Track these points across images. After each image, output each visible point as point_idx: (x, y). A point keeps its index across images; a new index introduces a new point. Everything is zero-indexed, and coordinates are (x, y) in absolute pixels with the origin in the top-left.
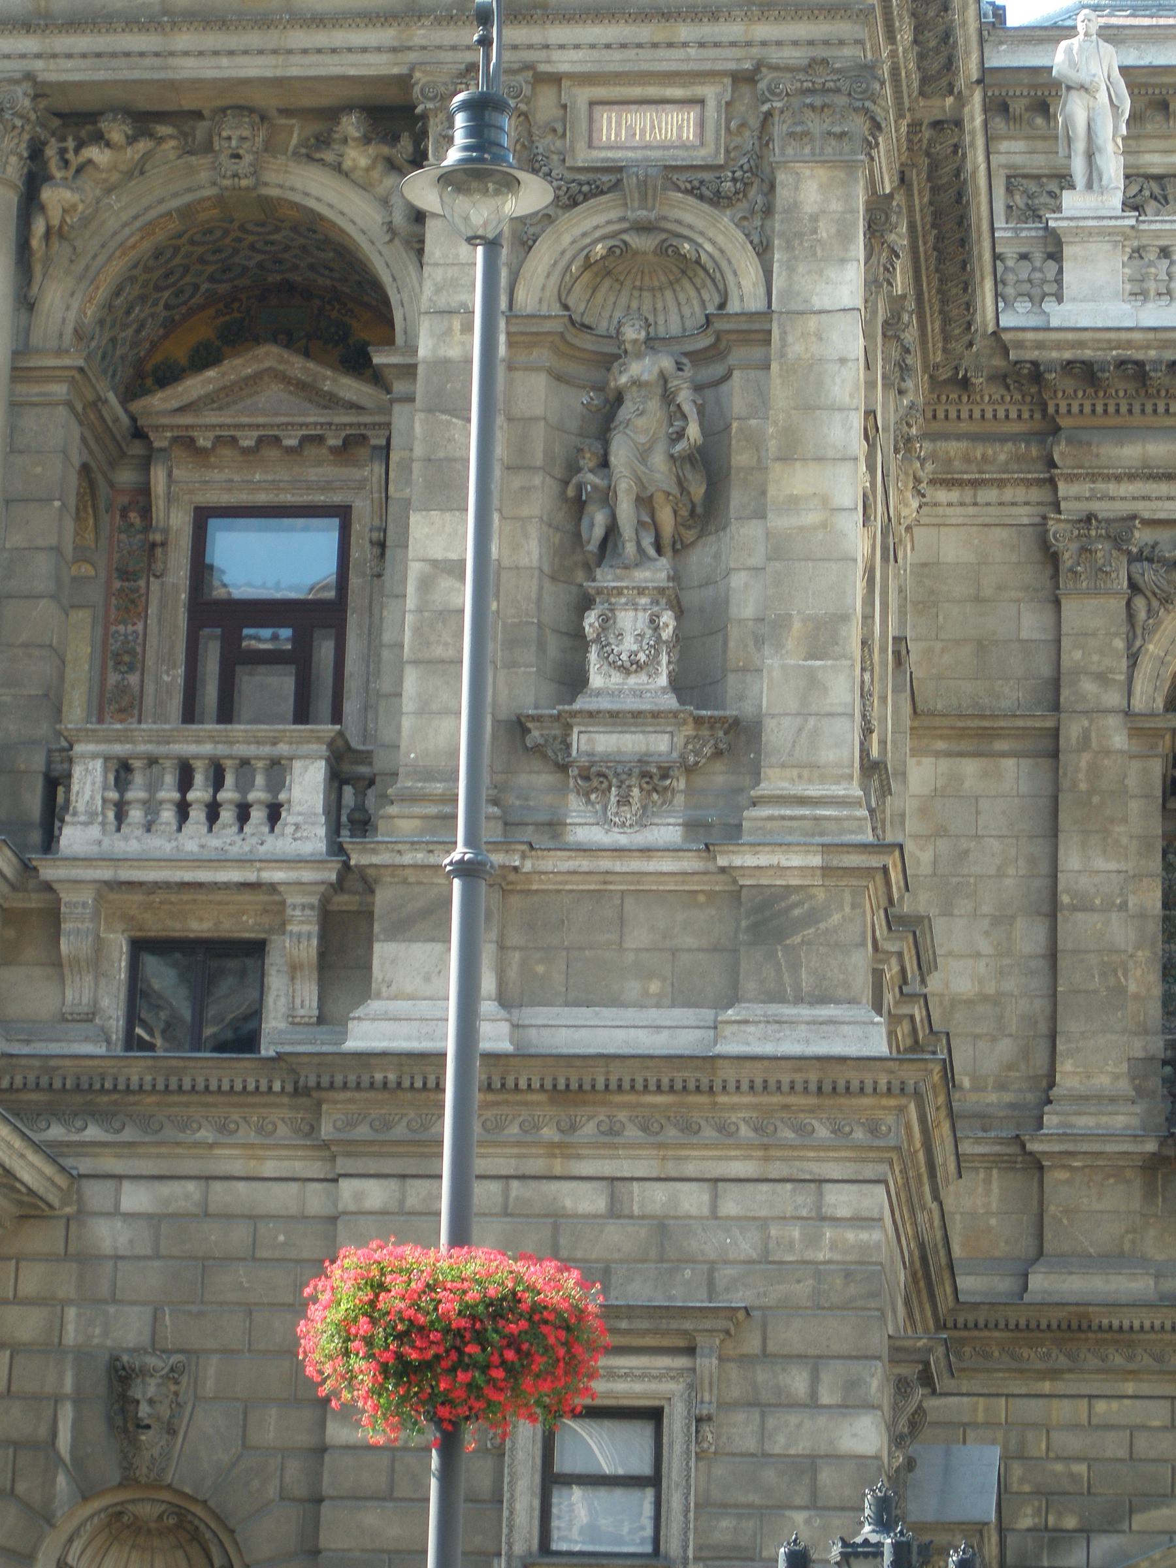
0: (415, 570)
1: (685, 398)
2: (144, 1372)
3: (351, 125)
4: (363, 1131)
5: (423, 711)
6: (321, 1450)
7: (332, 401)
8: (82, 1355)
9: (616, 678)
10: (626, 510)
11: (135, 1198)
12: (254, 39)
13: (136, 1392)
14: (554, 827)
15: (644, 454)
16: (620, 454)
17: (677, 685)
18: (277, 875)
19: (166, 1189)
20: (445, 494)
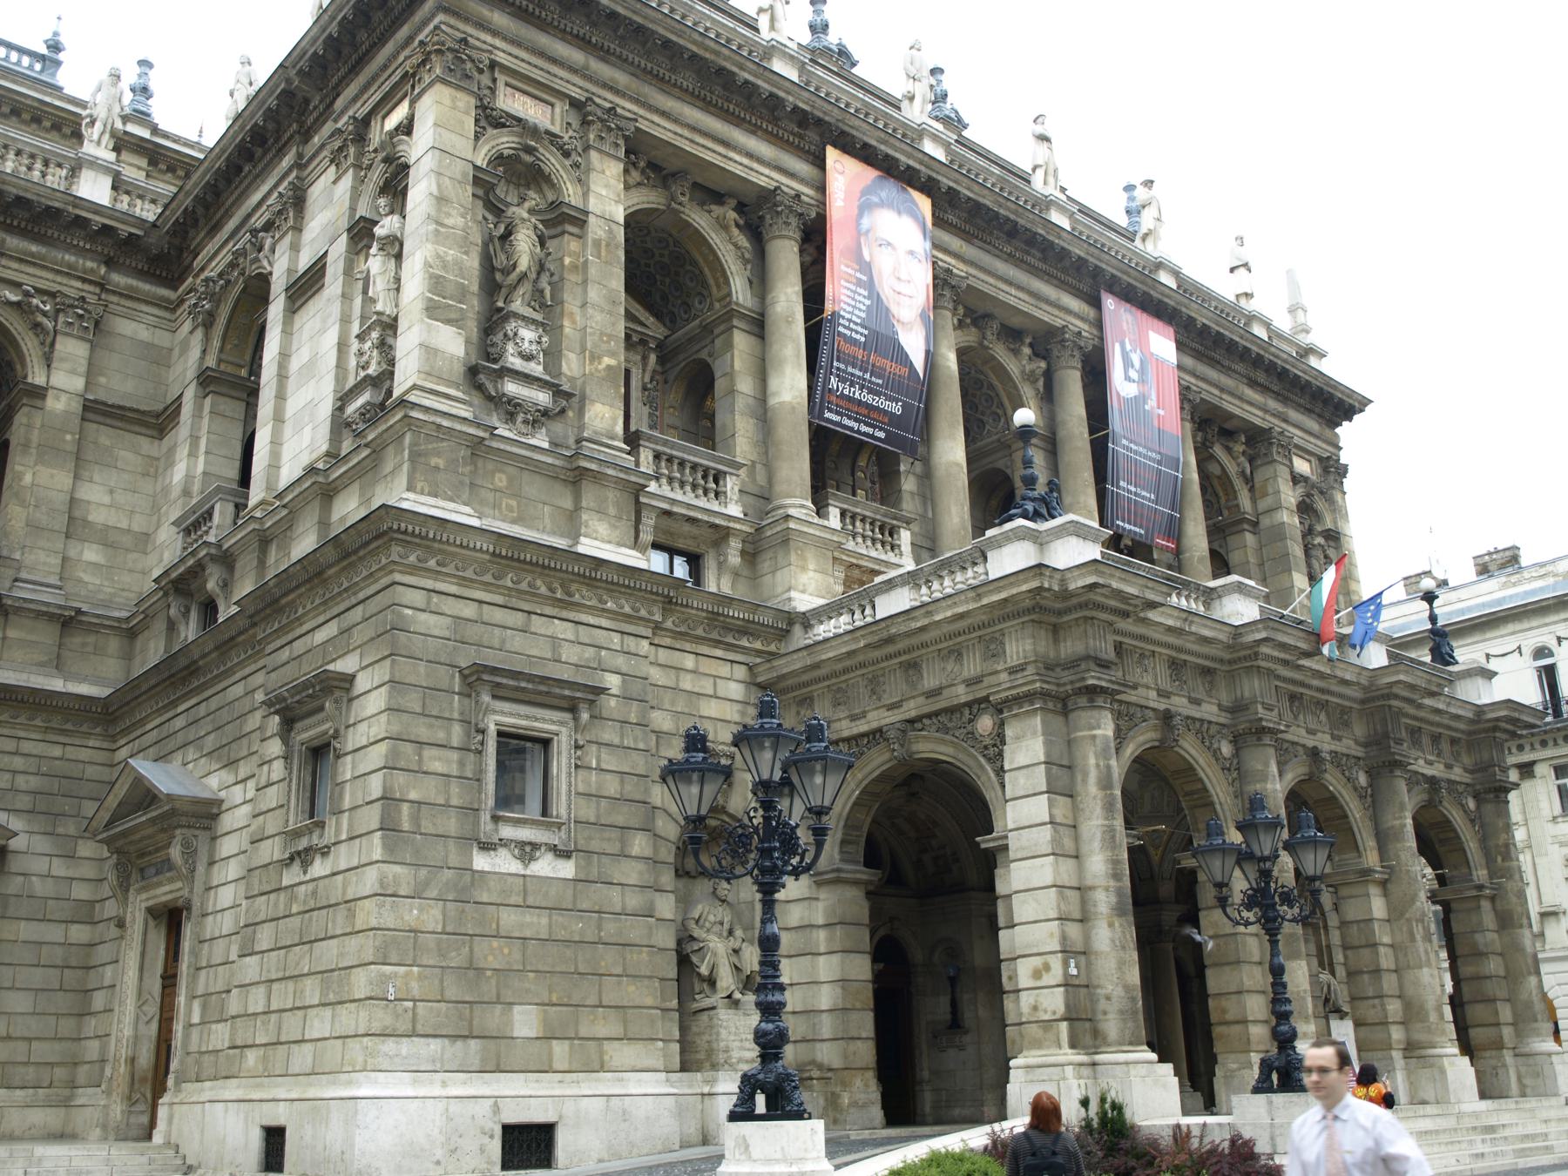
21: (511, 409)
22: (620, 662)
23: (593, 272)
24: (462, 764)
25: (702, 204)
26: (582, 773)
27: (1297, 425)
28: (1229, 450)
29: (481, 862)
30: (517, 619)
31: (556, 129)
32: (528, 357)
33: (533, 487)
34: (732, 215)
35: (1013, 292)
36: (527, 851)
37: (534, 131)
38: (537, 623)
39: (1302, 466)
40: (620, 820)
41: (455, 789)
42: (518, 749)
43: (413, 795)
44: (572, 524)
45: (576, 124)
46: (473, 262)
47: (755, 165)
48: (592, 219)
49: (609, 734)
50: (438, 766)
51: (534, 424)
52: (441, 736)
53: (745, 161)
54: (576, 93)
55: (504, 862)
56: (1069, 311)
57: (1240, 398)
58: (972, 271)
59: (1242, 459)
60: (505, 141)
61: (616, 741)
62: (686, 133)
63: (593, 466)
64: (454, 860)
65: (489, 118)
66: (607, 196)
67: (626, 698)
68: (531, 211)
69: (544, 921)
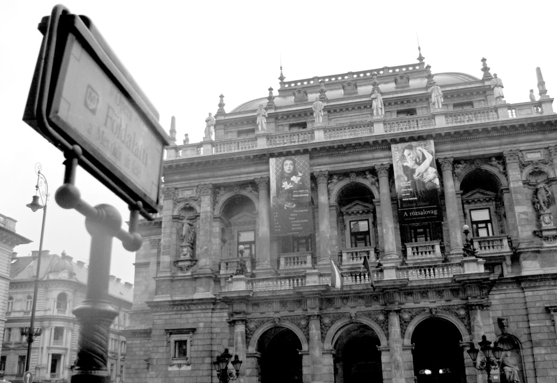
0: (517, 214)
1: (547, 189)
2: (504, 319)
3: (494, 159)
4: (527, 285)
5: (522, 231)
6: (529, 327)
7: (486, 194)
8: (493, 318)
9: (546, 225)
10: (542, 204)
11: (497, 297)
12: (481, 149)
13: (503, 322)
14: (542, 244)
15: (543, 196)
16: (539, 196)
17: (555, 225)
18: (505, 254)
19: (500, 295)
20: (519, 204)
21: (181, 269)
22: (204, 320)
23: (201, 227)
24: (166, 349)
25: (244, 189)
26: (193, 347)
27: (522, 143)
28: (492, 165)
29: (170, 369)
30: (179, 316)
31: (194, 195)
32: (185, 255)
33: (187, 284)
34: (250, 188)
35: (351, 164)
36: (180, 365)
37: (186, 200)
38: (183, 316)
39: (530, 157)
40: (202, 355)
41: (165, 355)
42: (181, 344)
43: (156, 357)
44: (195, 291)
45: (198, 190)
46: (174, 237)
47: (249, 175)
48: (201, 214)
49: (200, 337)
50: (161, 351)
51: (187, 270)
52: (162, 344)
53: (246, 175)
54: (197, 184)
55: (175, 368)
56: (379, 158)
57: (482, 147)
58: (332, 166)
59: (499, 166)
60: (182, 205)
61: (202, 338)
62: (227, 178)
63: (197, 276)
64: (164, 369)
65: (176, 202)
66: (205, 207)
67: (205, 327)
68: (188, 219)
69: (184, 379)
